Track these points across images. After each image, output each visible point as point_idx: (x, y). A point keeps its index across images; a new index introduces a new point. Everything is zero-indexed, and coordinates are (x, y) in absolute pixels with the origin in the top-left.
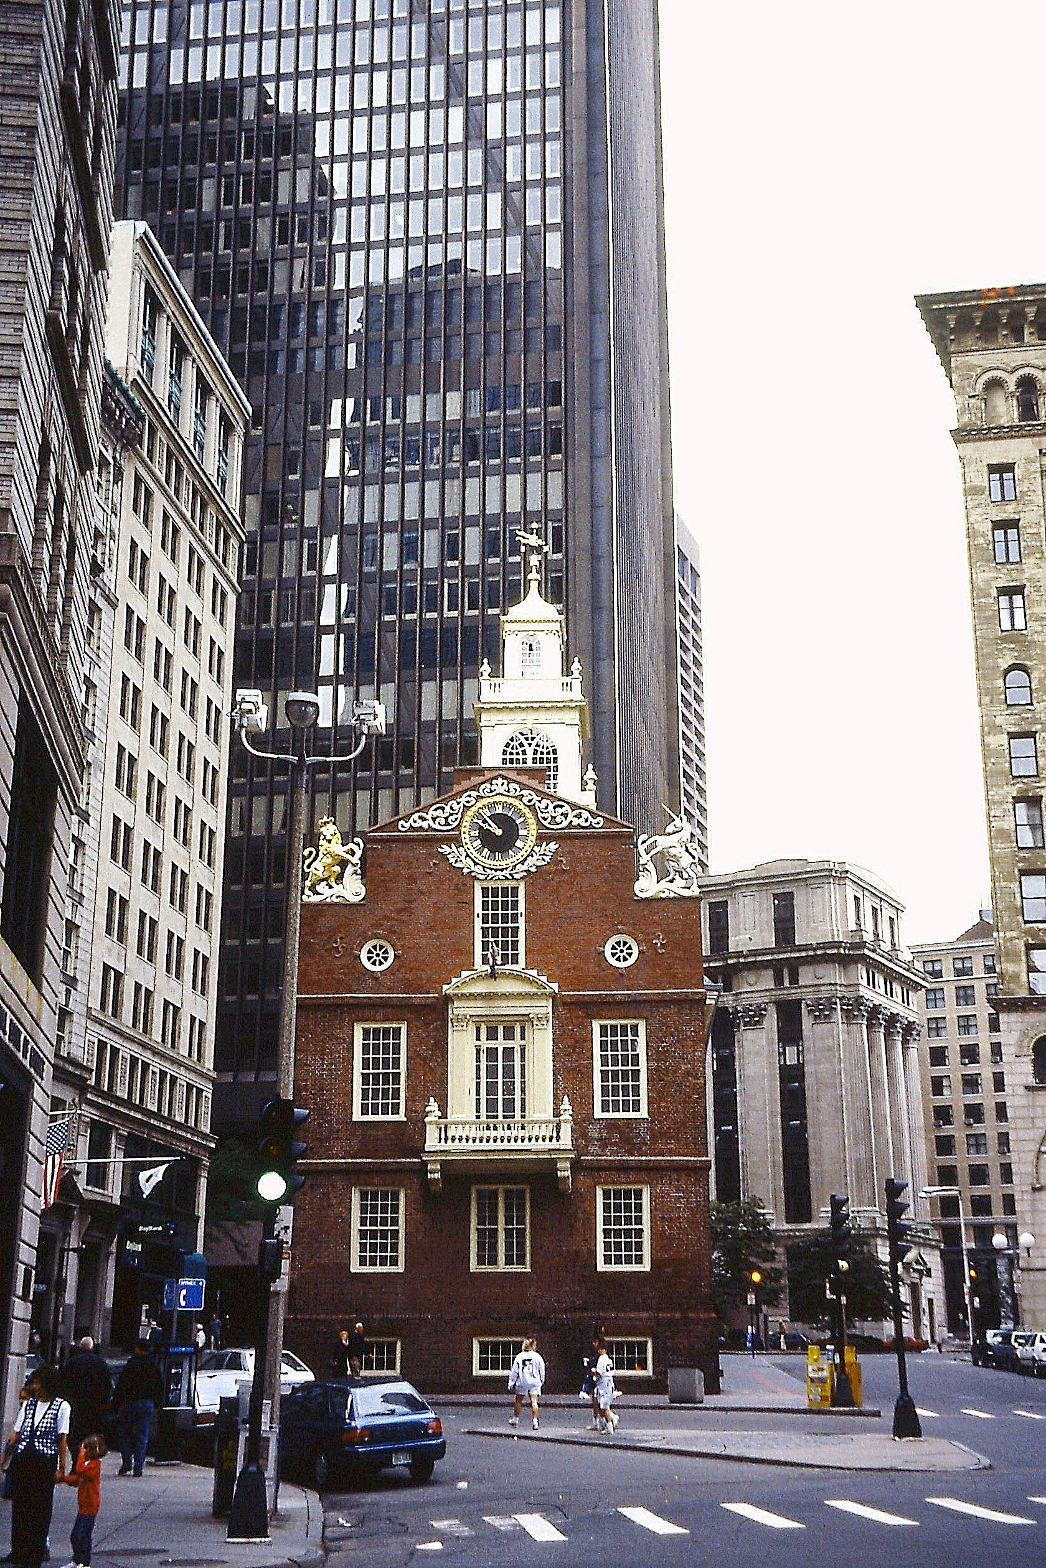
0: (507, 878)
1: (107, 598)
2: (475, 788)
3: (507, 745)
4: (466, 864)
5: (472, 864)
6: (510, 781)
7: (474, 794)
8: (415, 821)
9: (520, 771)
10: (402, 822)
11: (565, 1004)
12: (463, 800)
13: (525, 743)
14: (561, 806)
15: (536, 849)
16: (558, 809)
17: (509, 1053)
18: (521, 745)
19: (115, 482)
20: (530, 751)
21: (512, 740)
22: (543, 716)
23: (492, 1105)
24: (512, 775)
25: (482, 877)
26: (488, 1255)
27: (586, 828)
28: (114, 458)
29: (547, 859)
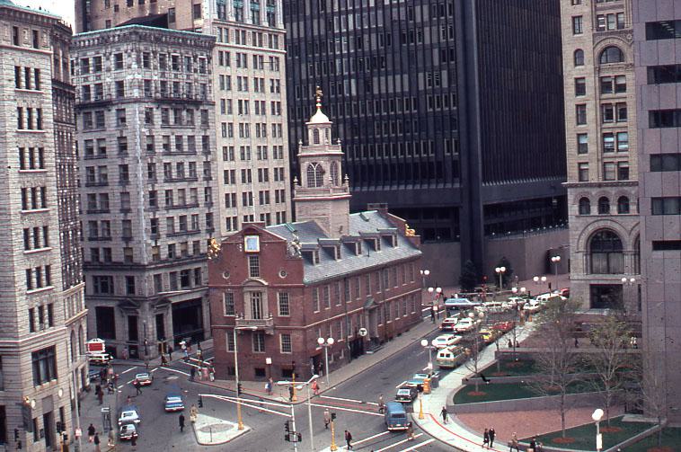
22: (317, 158)
26: (256, 350)
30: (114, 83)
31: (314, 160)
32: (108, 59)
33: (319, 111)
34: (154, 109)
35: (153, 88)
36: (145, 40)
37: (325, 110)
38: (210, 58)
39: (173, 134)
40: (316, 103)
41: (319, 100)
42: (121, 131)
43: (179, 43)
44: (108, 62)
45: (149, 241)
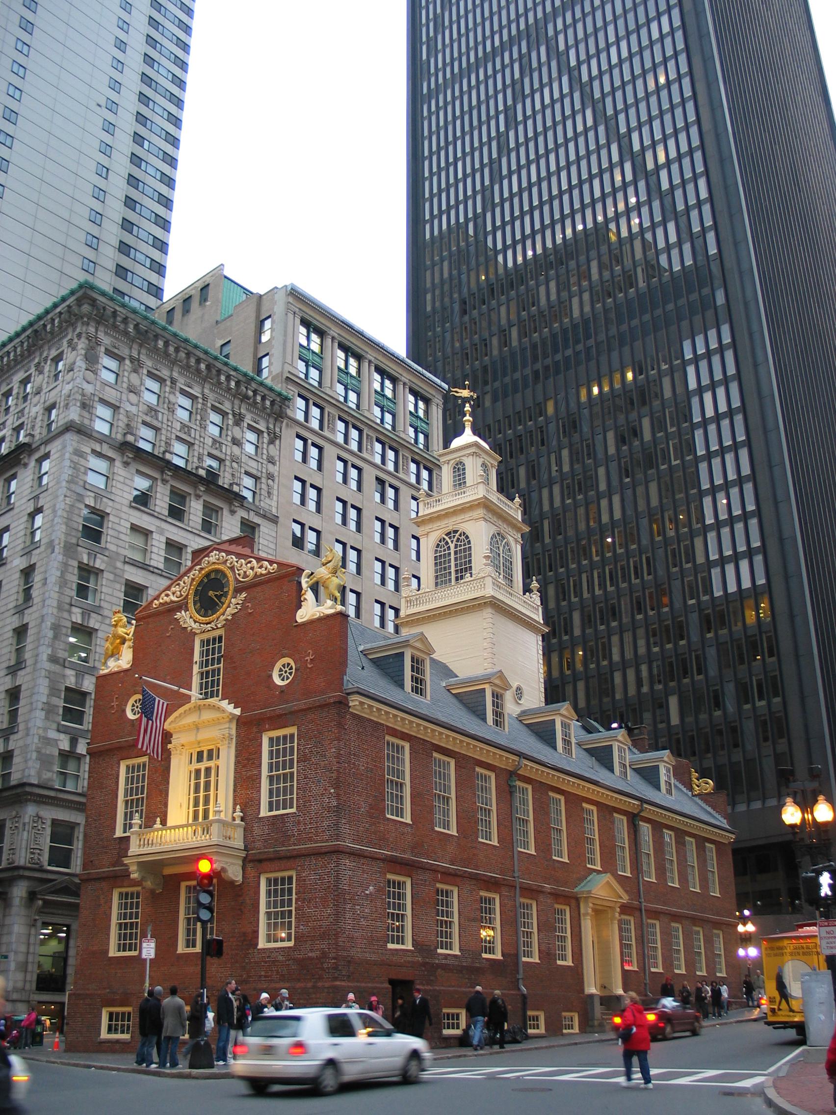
0: (214, 629)
1: (264, 517)
2: (199, 563)
3: (438, 546)
4: (191, 624)
5: (193, 624)
6: (220, 550)
7: (198, 567)
8: (164, 599)
9: (232, 541)
10: (156, 601)
11: (245, 724)
12: (191, 575)
13: (449, 541)
14: (250, 562)
15: (233, 600)
16: (249, 565)
17: (208, 770)
18: (447, 543)
19: (271, 442)
20: (452, 546)
21: (440, 541)
22: (459, 518)
23: (196, 817)
24: (225, 547)
25: (198, 631)
27: (266, 574)
28: (268, 428)
29: (239, 607)
30: (41, 411)
31: (450, 524)
32: (41, 372)
33: (468, 431)
34: (118, 463)
35: (121, 424)
36: (115, 327)
37: (475, 432)
38: (274, 438)
39: (161, 531)
40: (465, 415)
41: (467, 408)
42: (36, 498)
43: (198, 371)
44: (41, 376)
45: (52, 734)
